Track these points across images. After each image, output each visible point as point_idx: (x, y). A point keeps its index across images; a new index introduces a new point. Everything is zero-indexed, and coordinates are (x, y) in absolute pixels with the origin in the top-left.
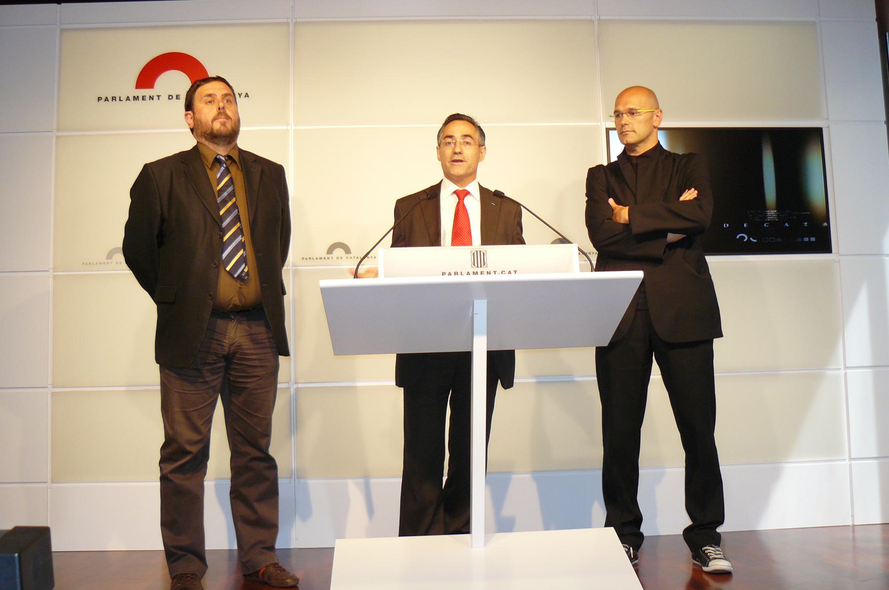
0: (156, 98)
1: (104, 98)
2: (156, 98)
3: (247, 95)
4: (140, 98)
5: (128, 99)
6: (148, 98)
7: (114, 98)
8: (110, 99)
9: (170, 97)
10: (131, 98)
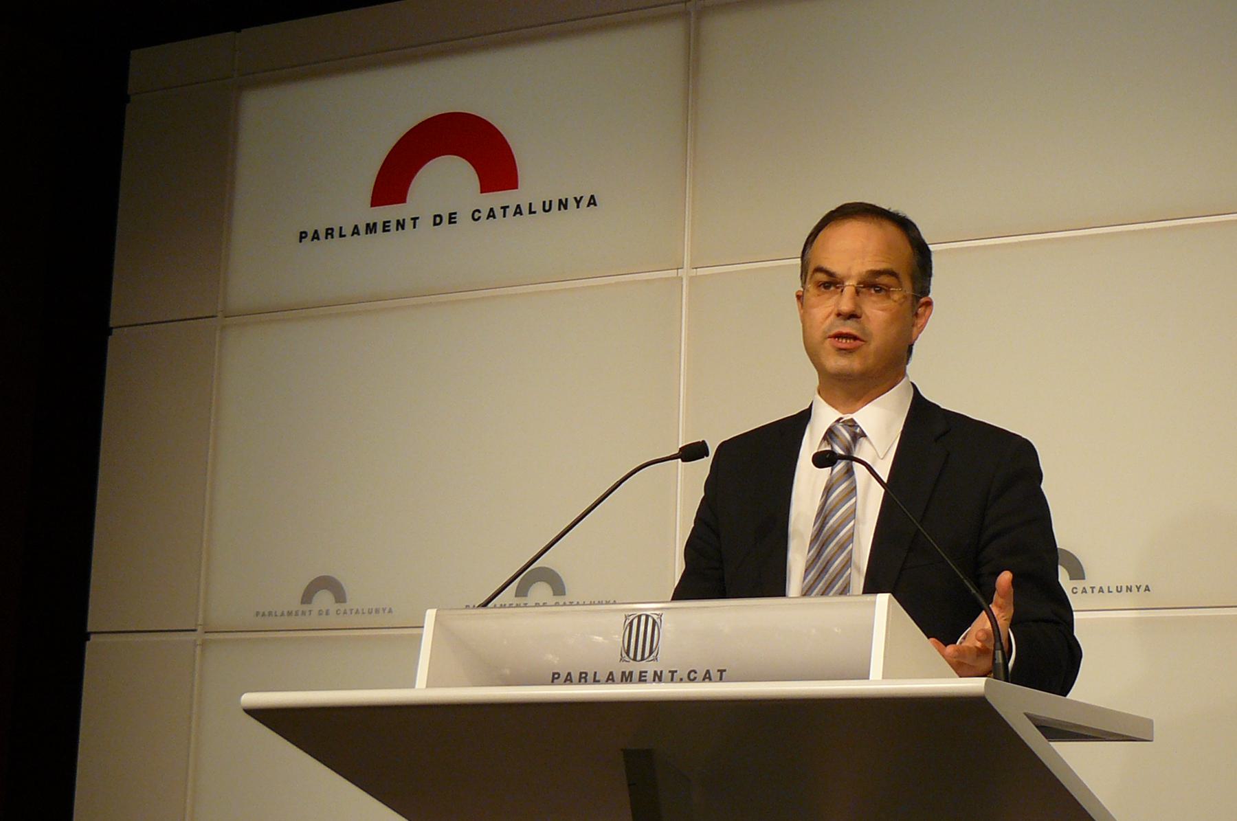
0: (409, 224)
1: (310, 235)
2: (409, 224)
3: (592, 201)
4: (380, 227)
5: (356, 231)
6: (393, 225)
7: (329, 232)
8: (322, 234)
9: (437, 220)
10: (362, 229)
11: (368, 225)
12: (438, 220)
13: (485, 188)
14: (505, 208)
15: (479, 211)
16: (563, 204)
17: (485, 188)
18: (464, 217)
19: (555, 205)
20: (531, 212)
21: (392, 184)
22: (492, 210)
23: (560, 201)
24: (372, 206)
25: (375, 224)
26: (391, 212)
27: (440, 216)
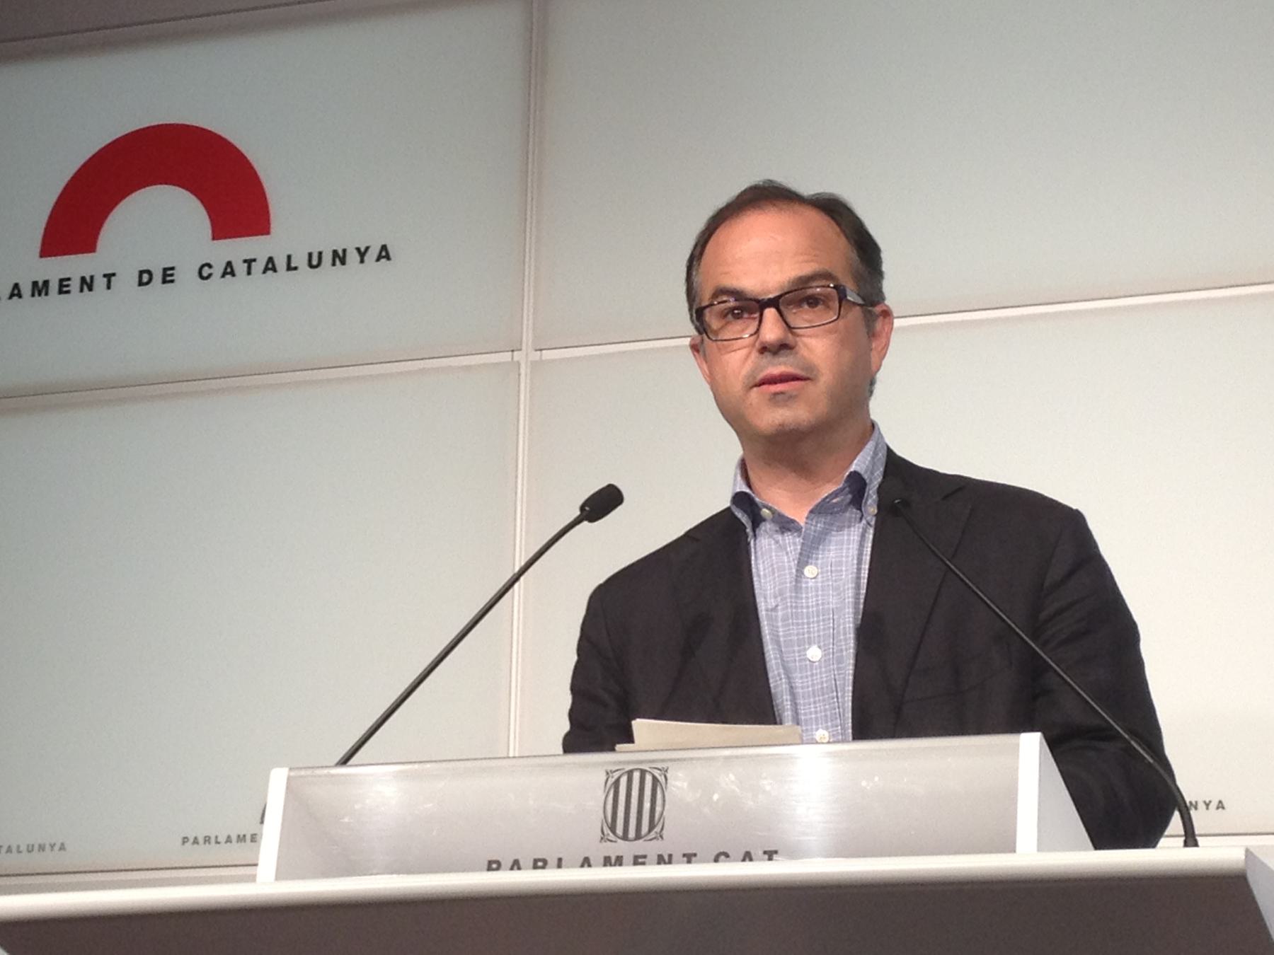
0: (100, 283)
2: (100, 283)
3: (384, 254)
4: (54, 286)
6: (75, 285)
9: (144, 278)
10: (26, 289)
11: (35, 284)
12: (145, 277)
13: (220, 232)
14: (249, 262)
15: (210, 266)
16: (339, 258)
17: (220, 232)
18: (185, 275)
19: (327, 258)
20: (289, 268)
21: (76, 220)
22: (229, 264)
23: (335, 253)
24: (41, 256)
25: (46, 283)
26: (74, 266)
27: (149, 272)
